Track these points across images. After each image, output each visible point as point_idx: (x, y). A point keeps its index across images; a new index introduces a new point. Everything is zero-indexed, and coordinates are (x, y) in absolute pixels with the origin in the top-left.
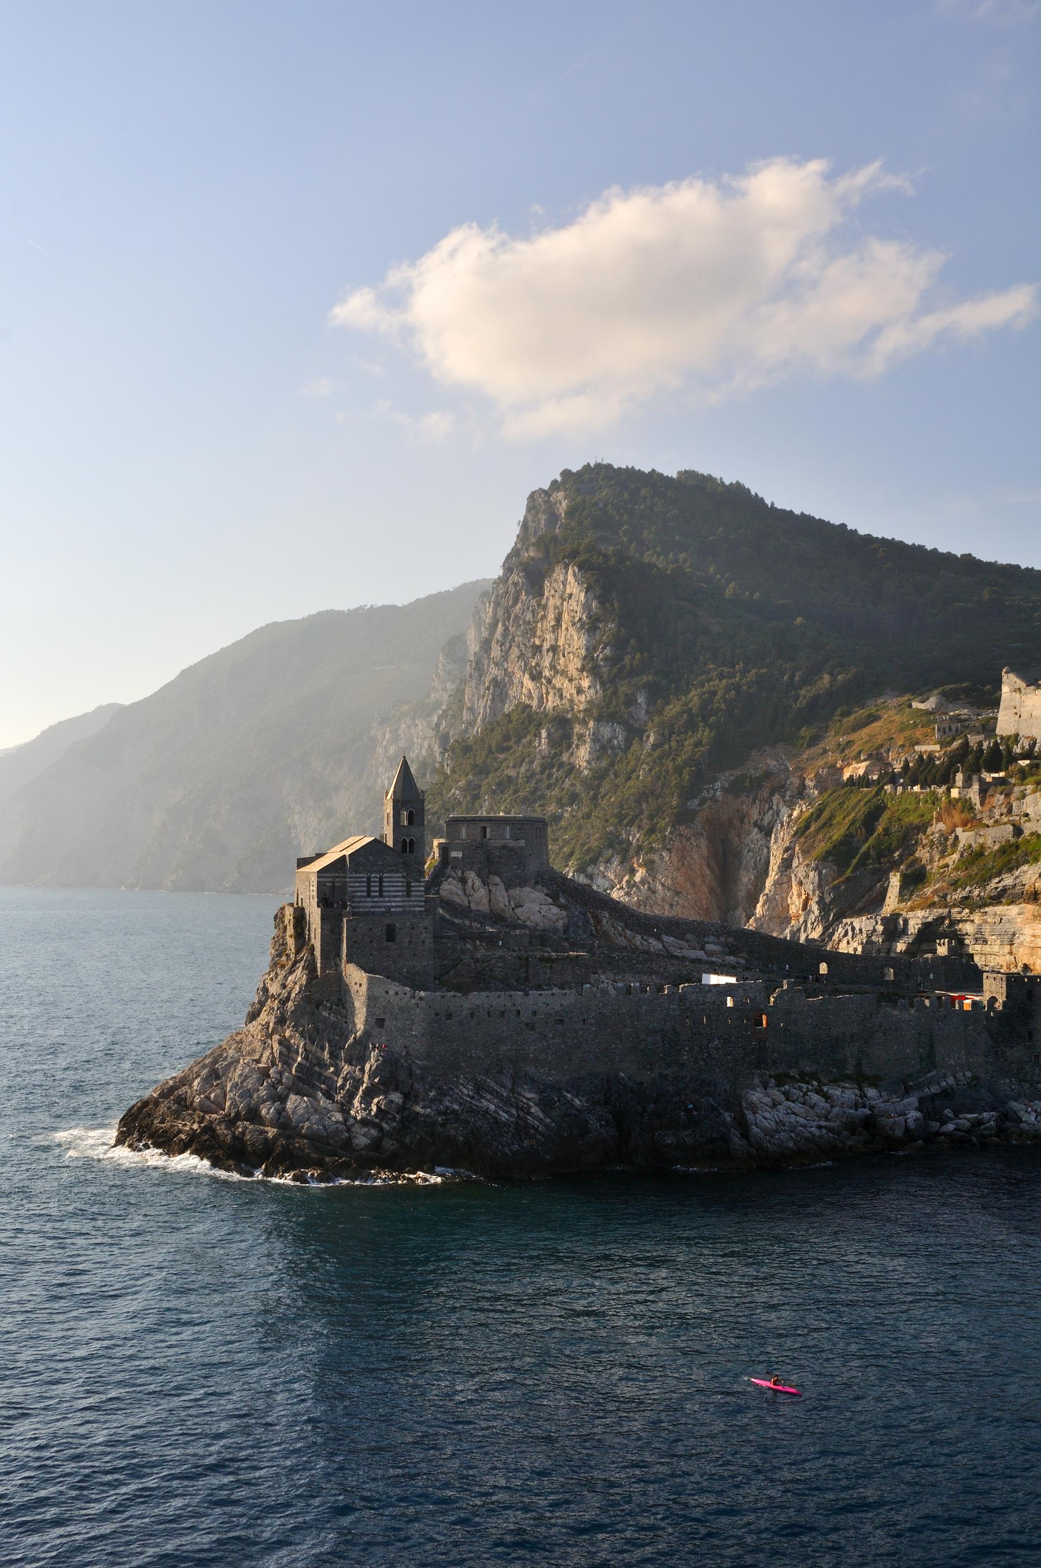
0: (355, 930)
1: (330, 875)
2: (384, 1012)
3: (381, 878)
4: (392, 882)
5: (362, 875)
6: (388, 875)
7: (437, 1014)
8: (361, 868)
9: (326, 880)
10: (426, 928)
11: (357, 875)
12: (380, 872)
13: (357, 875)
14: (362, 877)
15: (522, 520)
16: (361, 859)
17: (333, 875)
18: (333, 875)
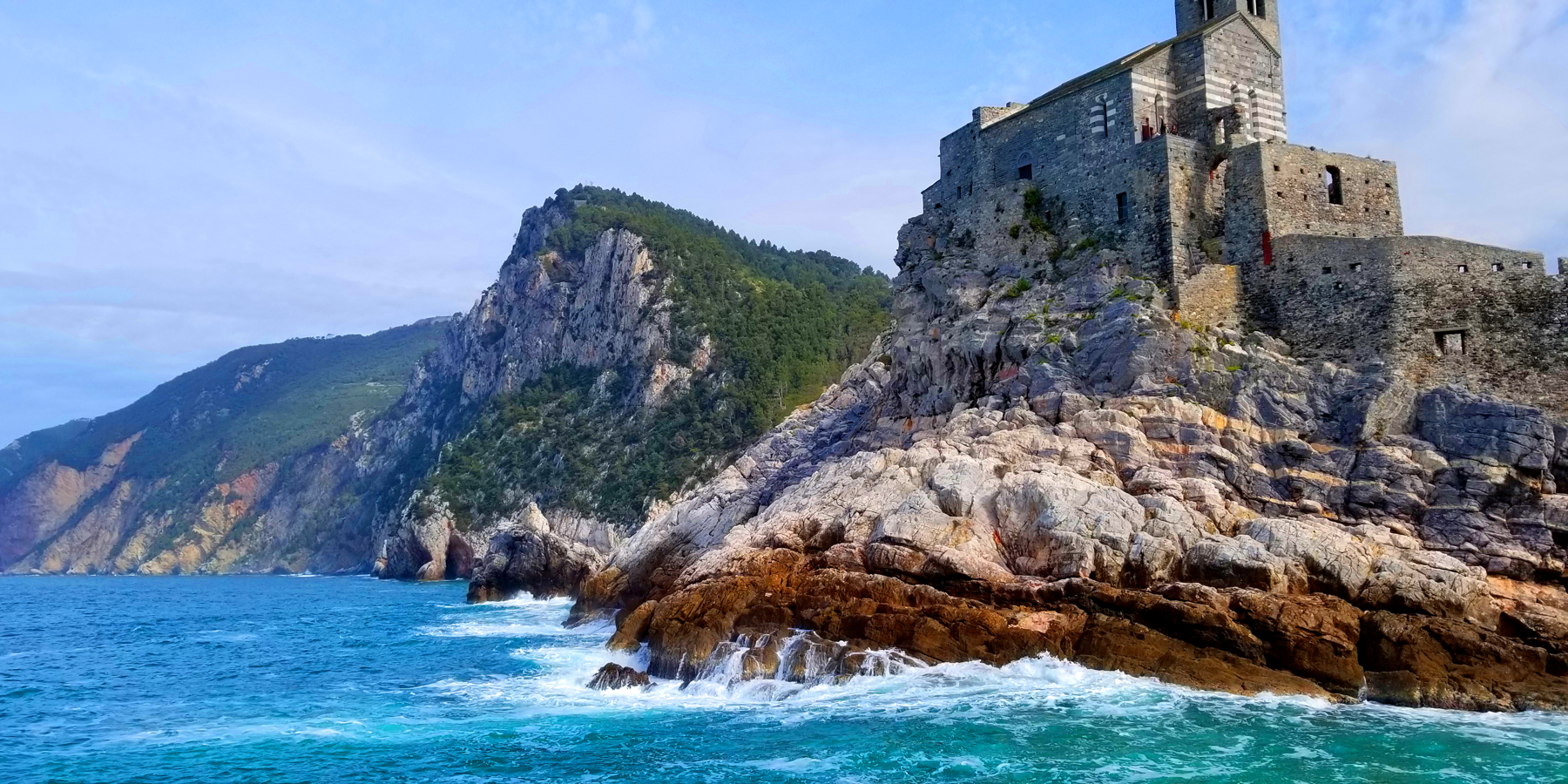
0: (1276, 168)
3: (1252, 94)
5: (1223, 81)
8: (1222, 66)
9: (1145, 89)
10: (1388, 186)
12: (1249, 81)
14: (1224, 86)
15: (518, 232)
16: (1222, 47)
17: (1157, 82)
18: (1157, 82)
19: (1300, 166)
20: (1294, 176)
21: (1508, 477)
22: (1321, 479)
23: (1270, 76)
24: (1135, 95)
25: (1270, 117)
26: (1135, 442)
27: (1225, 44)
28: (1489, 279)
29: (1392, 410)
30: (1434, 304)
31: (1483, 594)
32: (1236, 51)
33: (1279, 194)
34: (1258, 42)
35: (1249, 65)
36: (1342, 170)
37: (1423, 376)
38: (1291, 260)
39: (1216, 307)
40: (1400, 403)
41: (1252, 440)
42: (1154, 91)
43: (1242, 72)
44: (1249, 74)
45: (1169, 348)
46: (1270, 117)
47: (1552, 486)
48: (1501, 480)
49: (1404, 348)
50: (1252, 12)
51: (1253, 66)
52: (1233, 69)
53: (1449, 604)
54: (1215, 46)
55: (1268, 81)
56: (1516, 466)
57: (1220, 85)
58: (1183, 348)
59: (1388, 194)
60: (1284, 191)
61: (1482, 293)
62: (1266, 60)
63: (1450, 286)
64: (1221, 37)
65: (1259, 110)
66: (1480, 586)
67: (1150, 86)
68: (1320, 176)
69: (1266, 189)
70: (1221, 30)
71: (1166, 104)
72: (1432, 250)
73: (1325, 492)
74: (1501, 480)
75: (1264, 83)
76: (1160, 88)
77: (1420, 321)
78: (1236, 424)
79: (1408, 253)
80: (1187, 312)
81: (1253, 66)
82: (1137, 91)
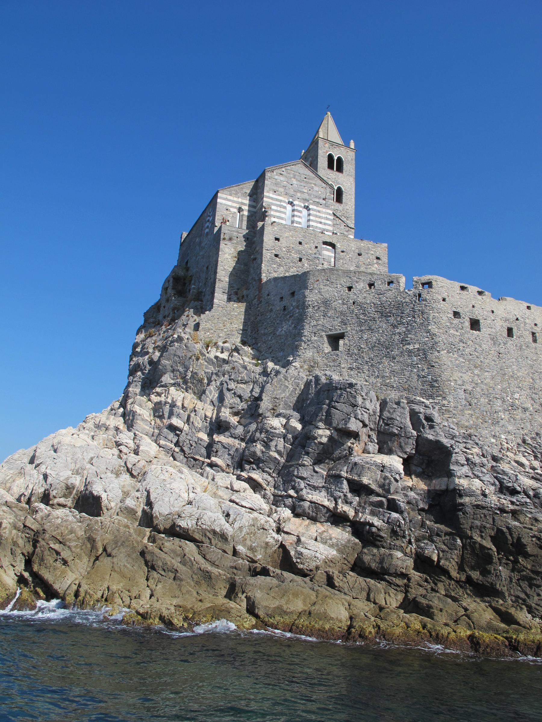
1: (235, 199)
2: (344, 323)
4: (320, 217)
6: (315, 207)
7: (456, 314)
8: (281, 190)
9: (230, 203)
10: (378, 258)
11: (275, 196)
12: (306, 200)
13: (275, 196)
16: (282, 178)
17: (240, 200)
18: (240, 200)
19: (299, 240)
20: (292, 245)
21: (330, 438)
22: (230, 443)
23: (324, 199)
24: (218, 206)
25: (321, 223)
26: (139, 417)
27: (286, 177)
28: (365, 295)
29: (284, 391)
30: (329, 315)
31: (263, 529)
32: (294, 182)
33: (276, 256)
34: (316, 179)
35: (306, 191)
36: (338, 245)
37: (313, 367)
38: (268, 295)
39: (226, 330)
40: (290, 386)
41: (206, 416)
42: (238, 206)
43: (299, 195)
44: (306, 196)
45: (181, 355)
46: (321, 223)
47: (373, 447)
48: (325, 440)
49: (306, 347)
50: (332, 169)
51: (310, 192)
52: (291, 192)
53: (214, 532)
54: (276, 177)
55: (324, 202)
56: (336, 429)
57: (277, 200)
58: (189, 355)
59: (377, 263)
60: (281, 254)
61: (359, 305)
62: (323, 190)
63: (340, 302)
64: (283, 173)
65: (311, 218)
66: (263, 522)
67: (233, 202)
68: (316, 247)
69: (264, 251)
70: (283, 169)
71: (246, 213)
72: (333, 278)
73: (231, 452)
74: (325, 440)
75: (318, 203)
76: (243, 204)
77: (319, 327)
78: (199, 405)
79: (318, 281)
80: (203, 332)
81: (310, 192)
82: (221, 204)
